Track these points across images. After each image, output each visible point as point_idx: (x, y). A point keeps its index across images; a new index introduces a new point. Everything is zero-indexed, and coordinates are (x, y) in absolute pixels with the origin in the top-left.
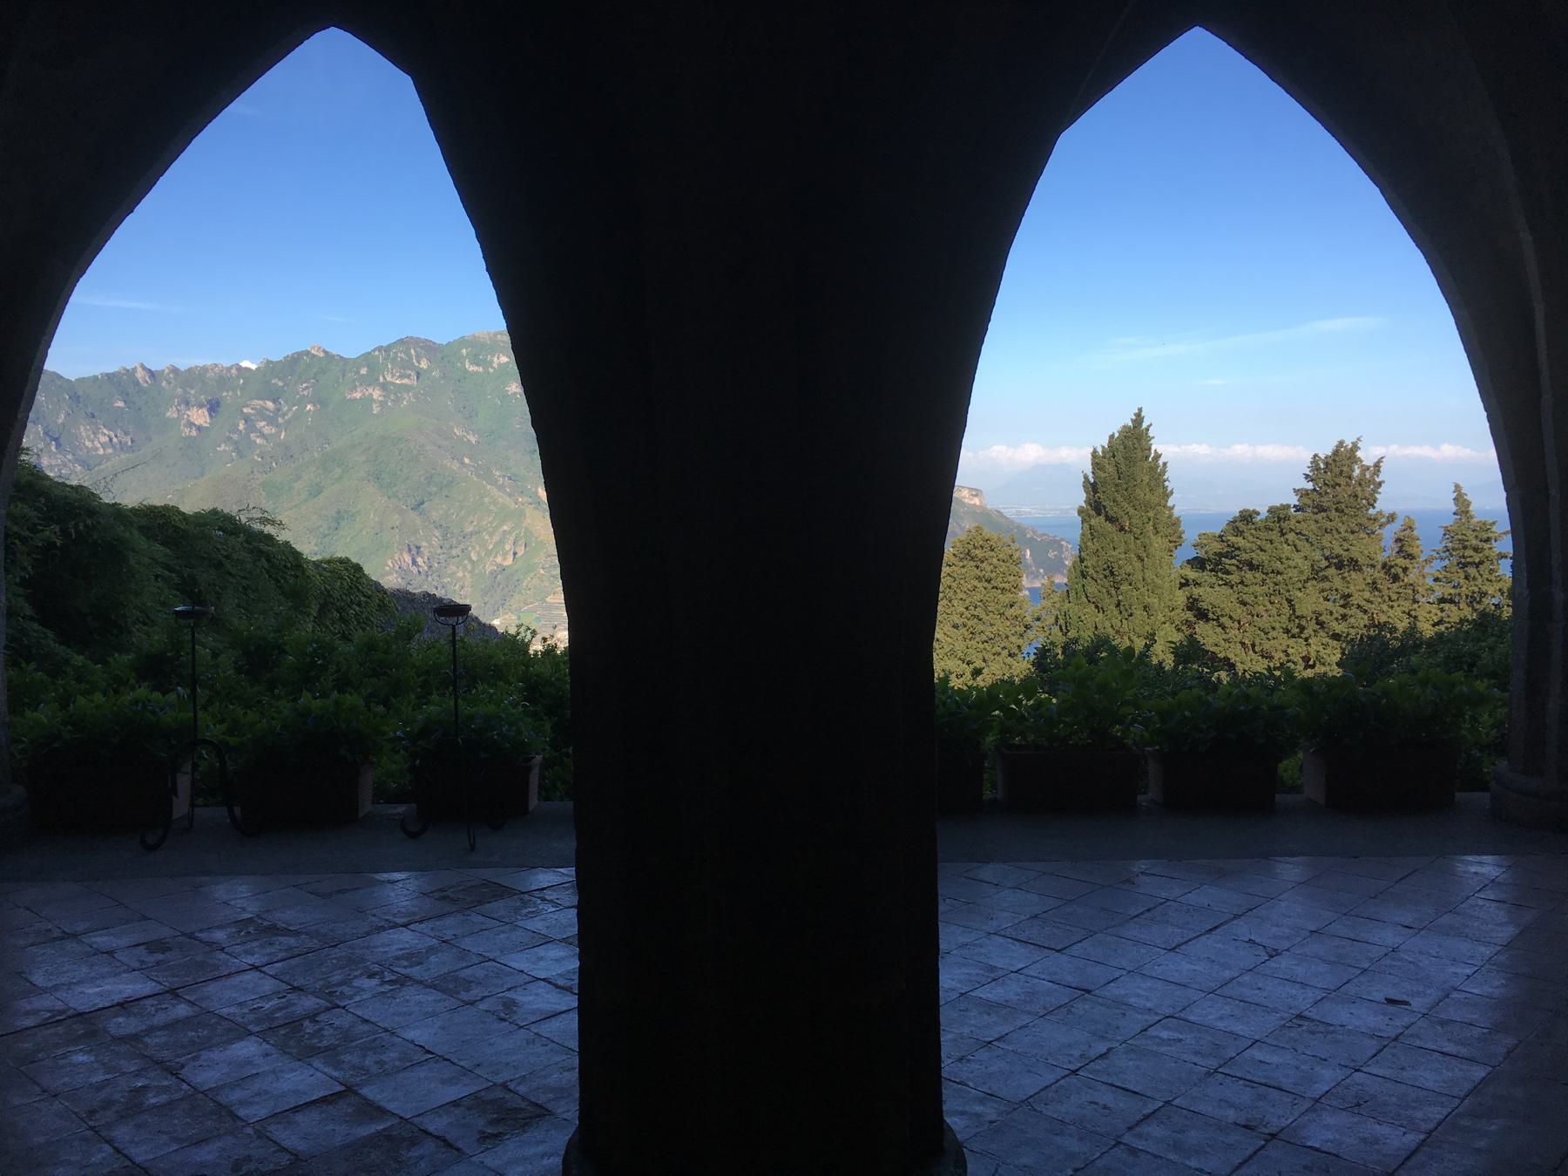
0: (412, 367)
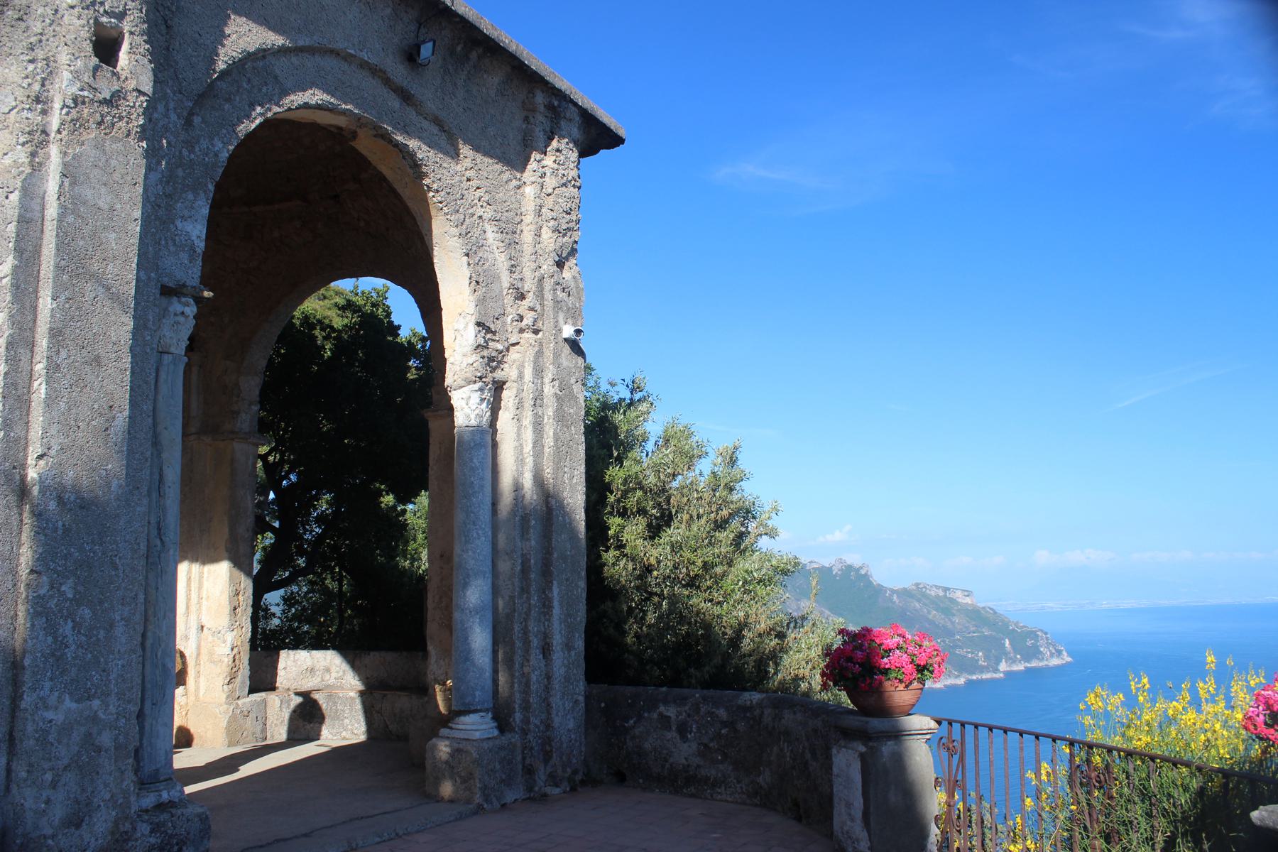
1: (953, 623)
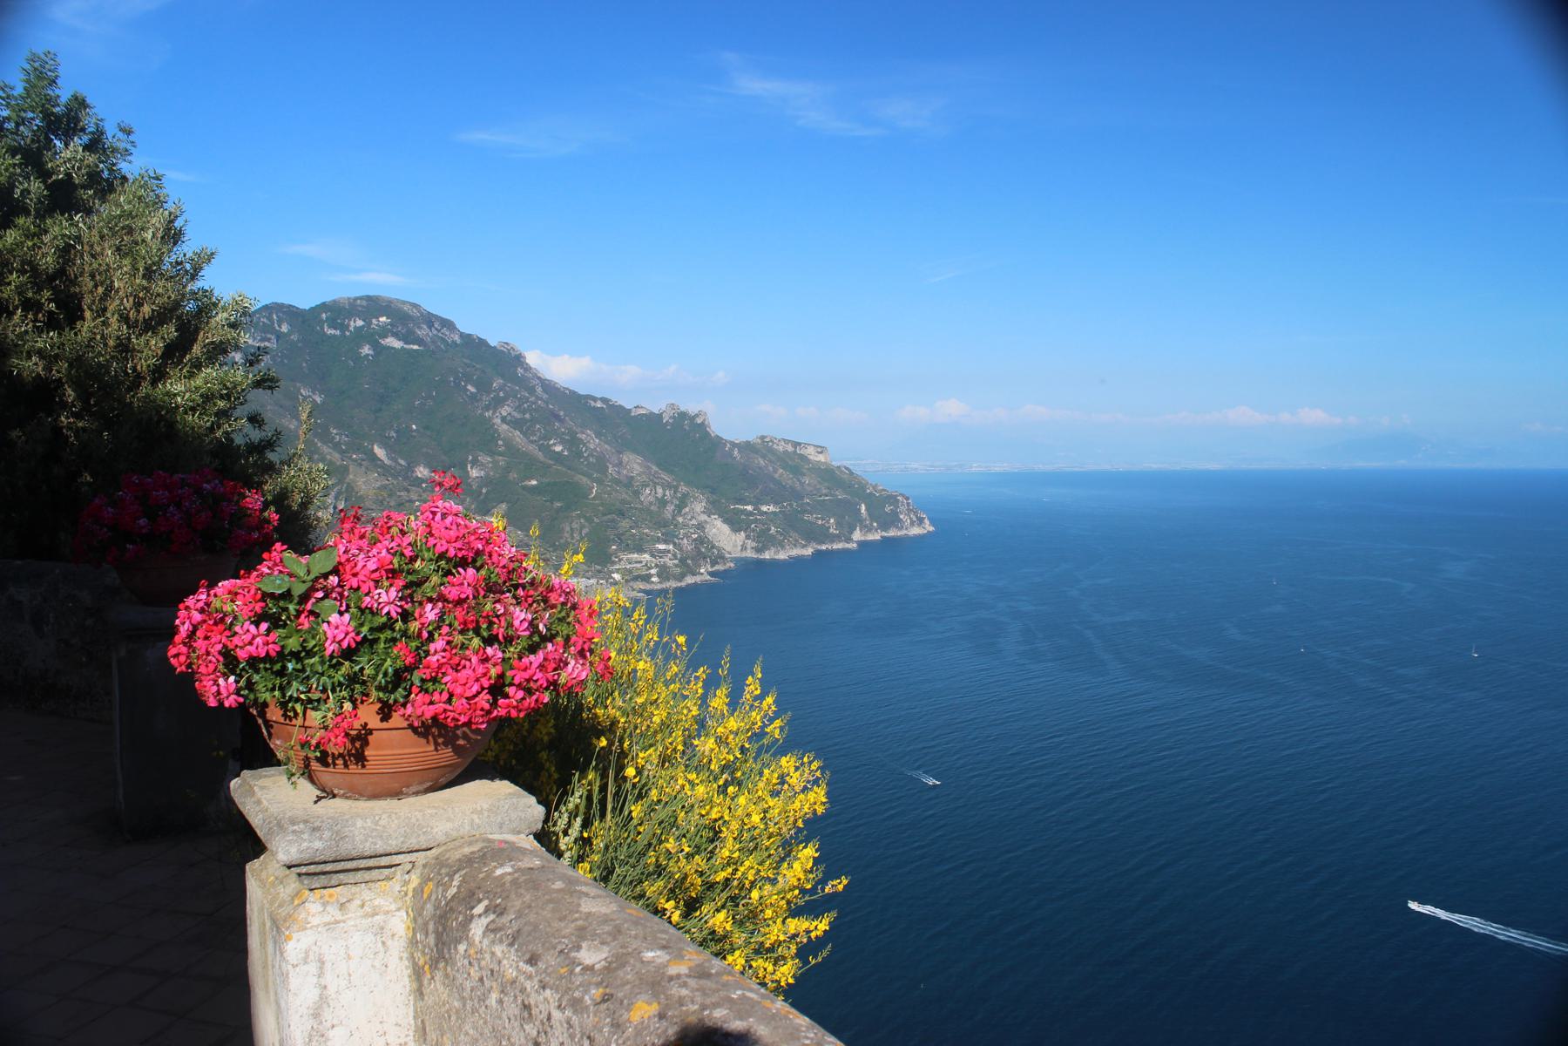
0: (274, 332)
1: (802, 484)
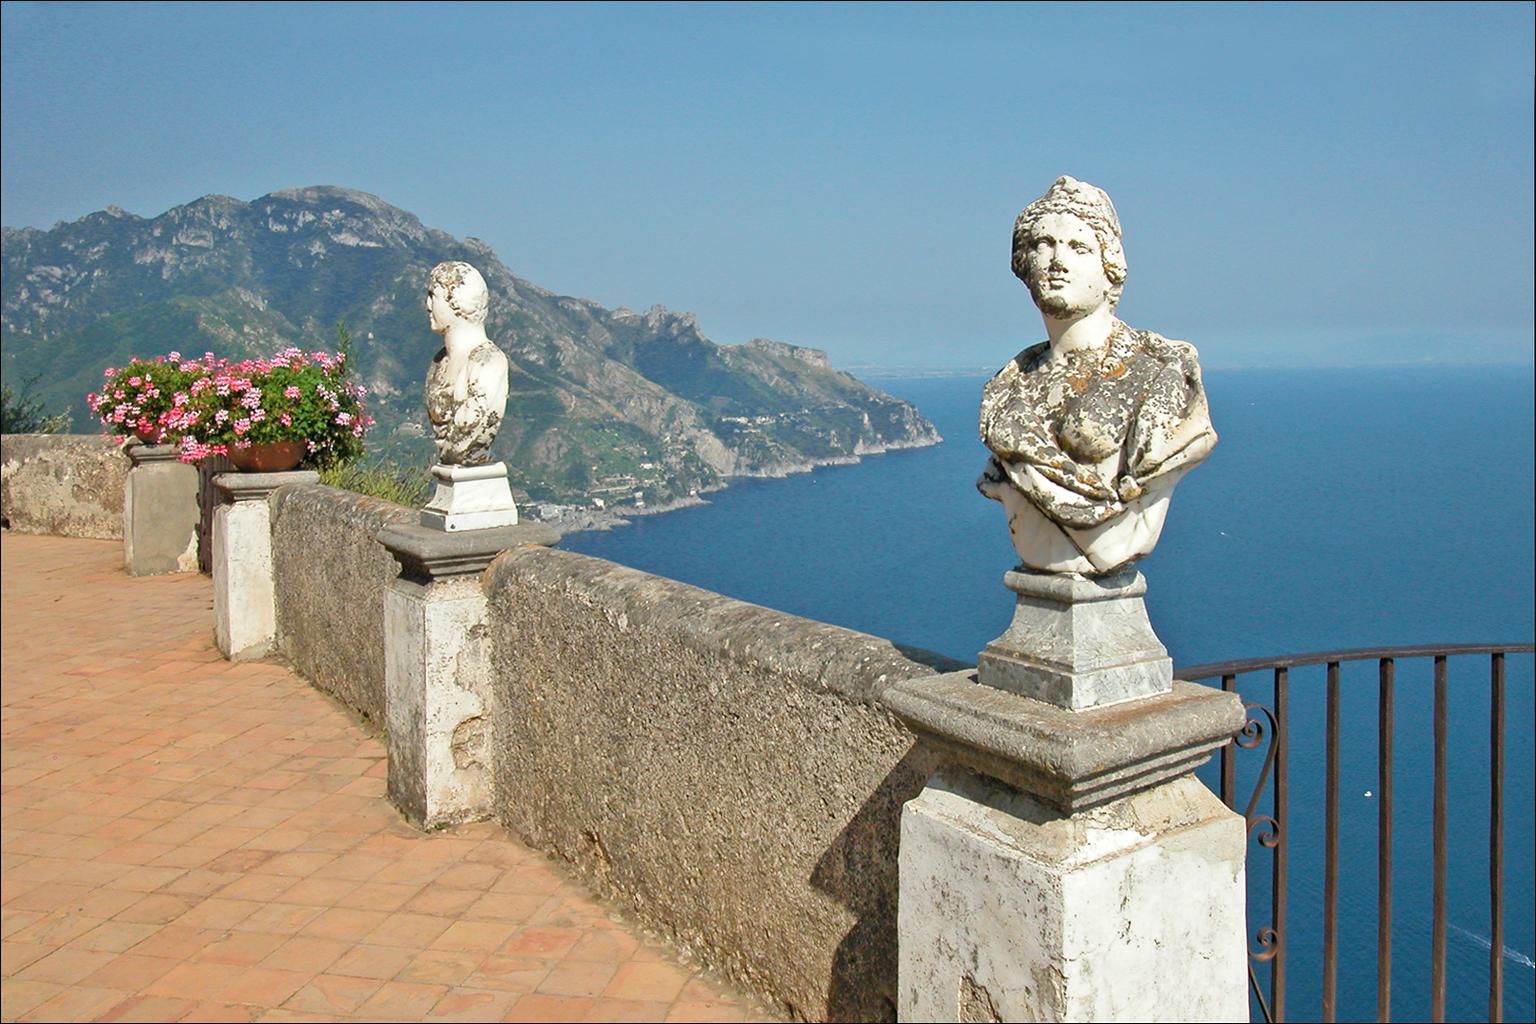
1: (800, 392)
